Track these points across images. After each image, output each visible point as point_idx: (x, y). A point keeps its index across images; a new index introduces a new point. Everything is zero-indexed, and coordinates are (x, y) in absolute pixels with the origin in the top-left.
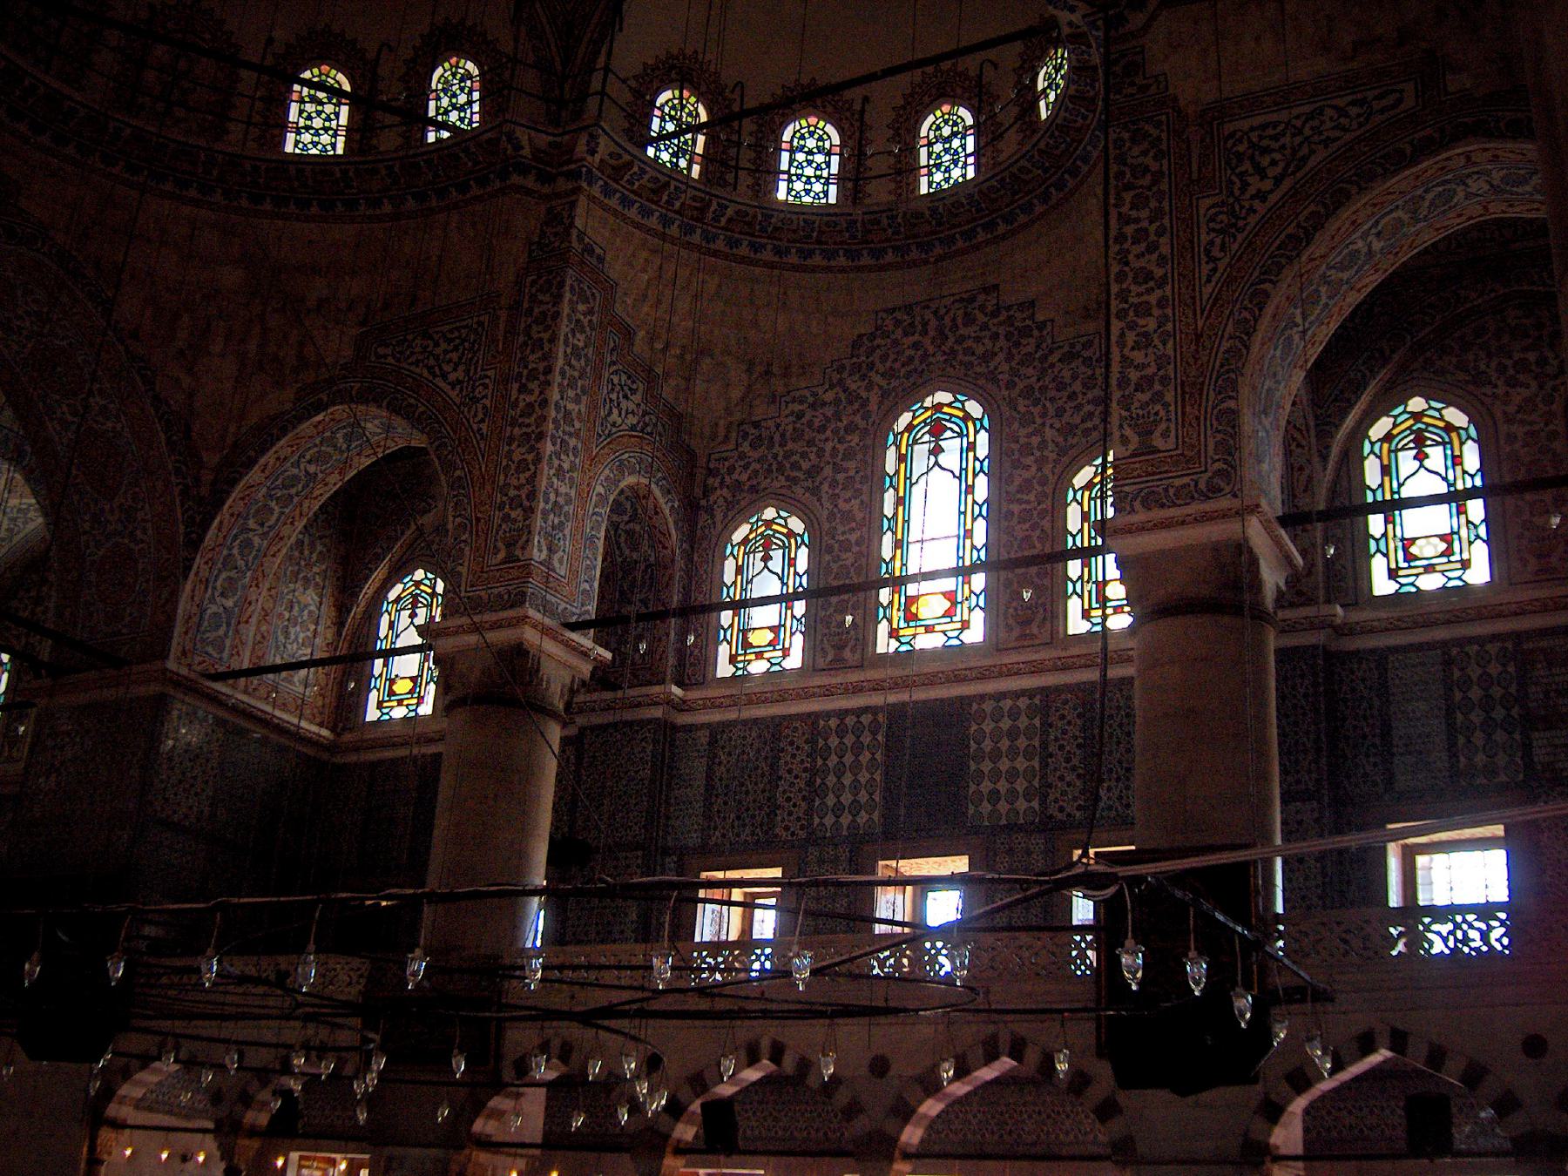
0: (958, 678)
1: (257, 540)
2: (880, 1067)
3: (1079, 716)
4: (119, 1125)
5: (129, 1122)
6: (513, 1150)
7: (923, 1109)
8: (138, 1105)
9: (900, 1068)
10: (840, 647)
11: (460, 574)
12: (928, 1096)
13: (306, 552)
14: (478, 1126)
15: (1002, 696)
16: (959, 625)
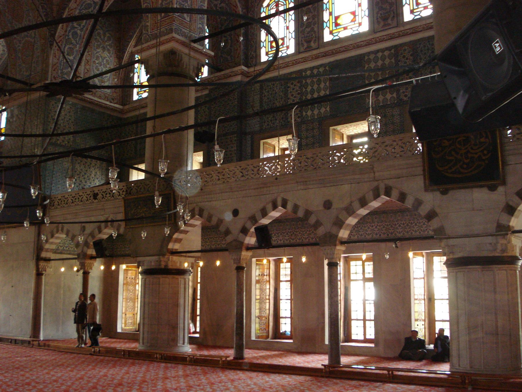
0: (358, 46)
1: (79, 32)
2: (328, 205)
3: (411, 55)
4: (48, 260)
5: (52, 258)
6: (184, 254)
7: (347, 222)
8: (55, 252)
9: (337, 205)
10: (309, 42)
11: (148, 26)
12: (350, 216)
13: (102, 37)
14: (171, 246)
15: (378, 51)
16: (358, 25)
